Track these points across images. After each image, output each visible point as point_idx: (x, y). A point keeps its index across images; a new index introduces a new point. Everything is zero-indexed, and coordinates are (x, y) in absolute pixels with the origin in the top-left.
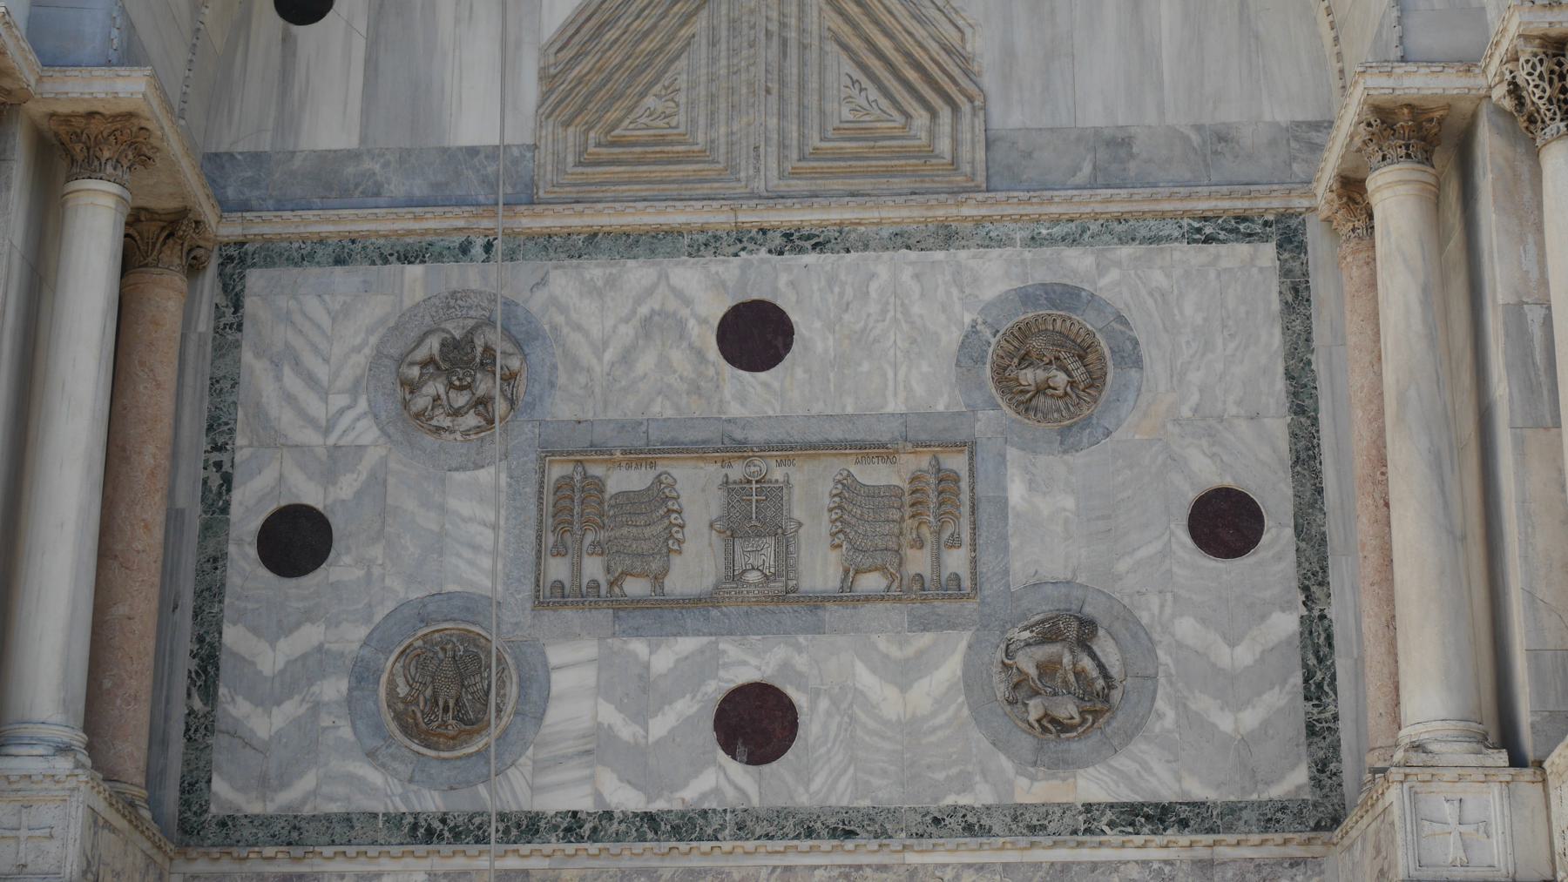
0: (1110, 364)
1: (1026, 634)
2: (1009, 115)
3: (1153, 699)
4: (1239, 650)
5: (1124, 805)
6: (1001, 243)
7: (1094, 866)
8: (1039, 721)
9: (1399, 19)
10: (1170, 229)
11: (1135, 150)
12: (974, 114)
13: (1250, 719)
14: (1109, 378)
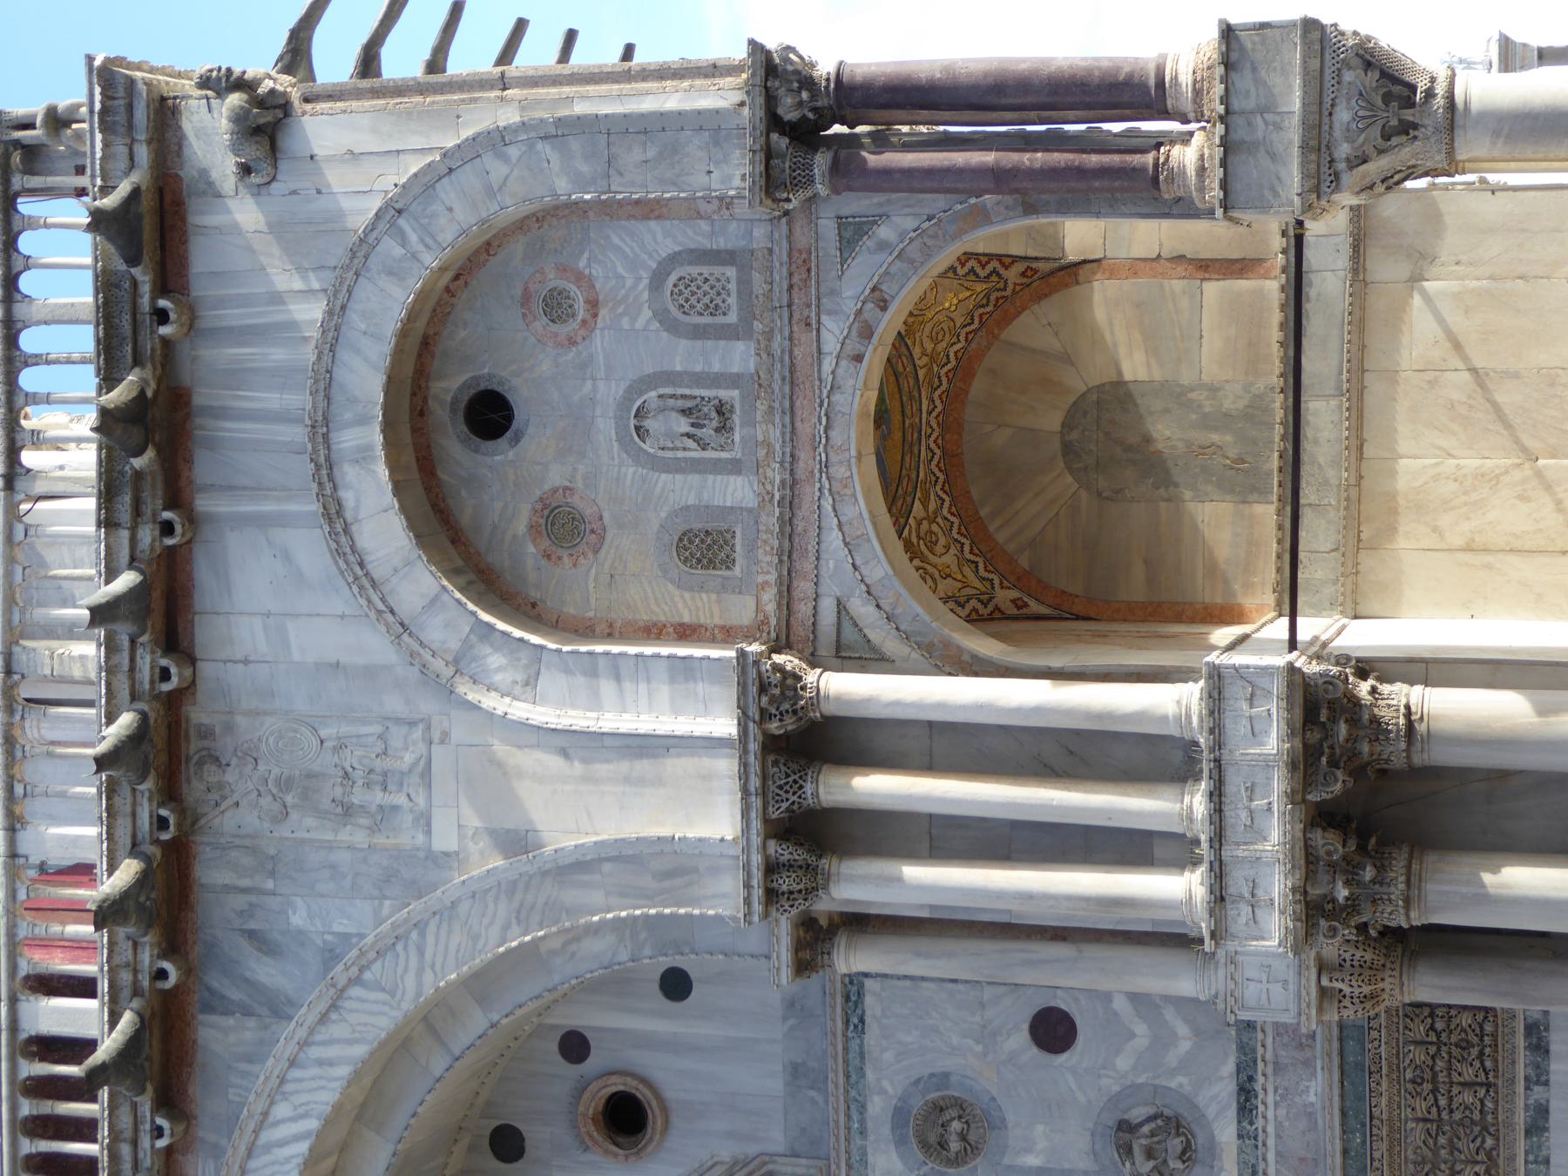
0: (946, 1093)
1: (1128, 1164)
2: (776, 1140)
3: (1170, 1089)
4: (1137, 1031)
5: (1238, 1113)
6: (864, 1154)
7: (1278, 1136)
8: (1184, 1162)
9: (739, 955)
10: (854, 1045)
11: (800, 1061)
12: (774, 1162)
13: (1182, 1030)
14: (956, 1094)
